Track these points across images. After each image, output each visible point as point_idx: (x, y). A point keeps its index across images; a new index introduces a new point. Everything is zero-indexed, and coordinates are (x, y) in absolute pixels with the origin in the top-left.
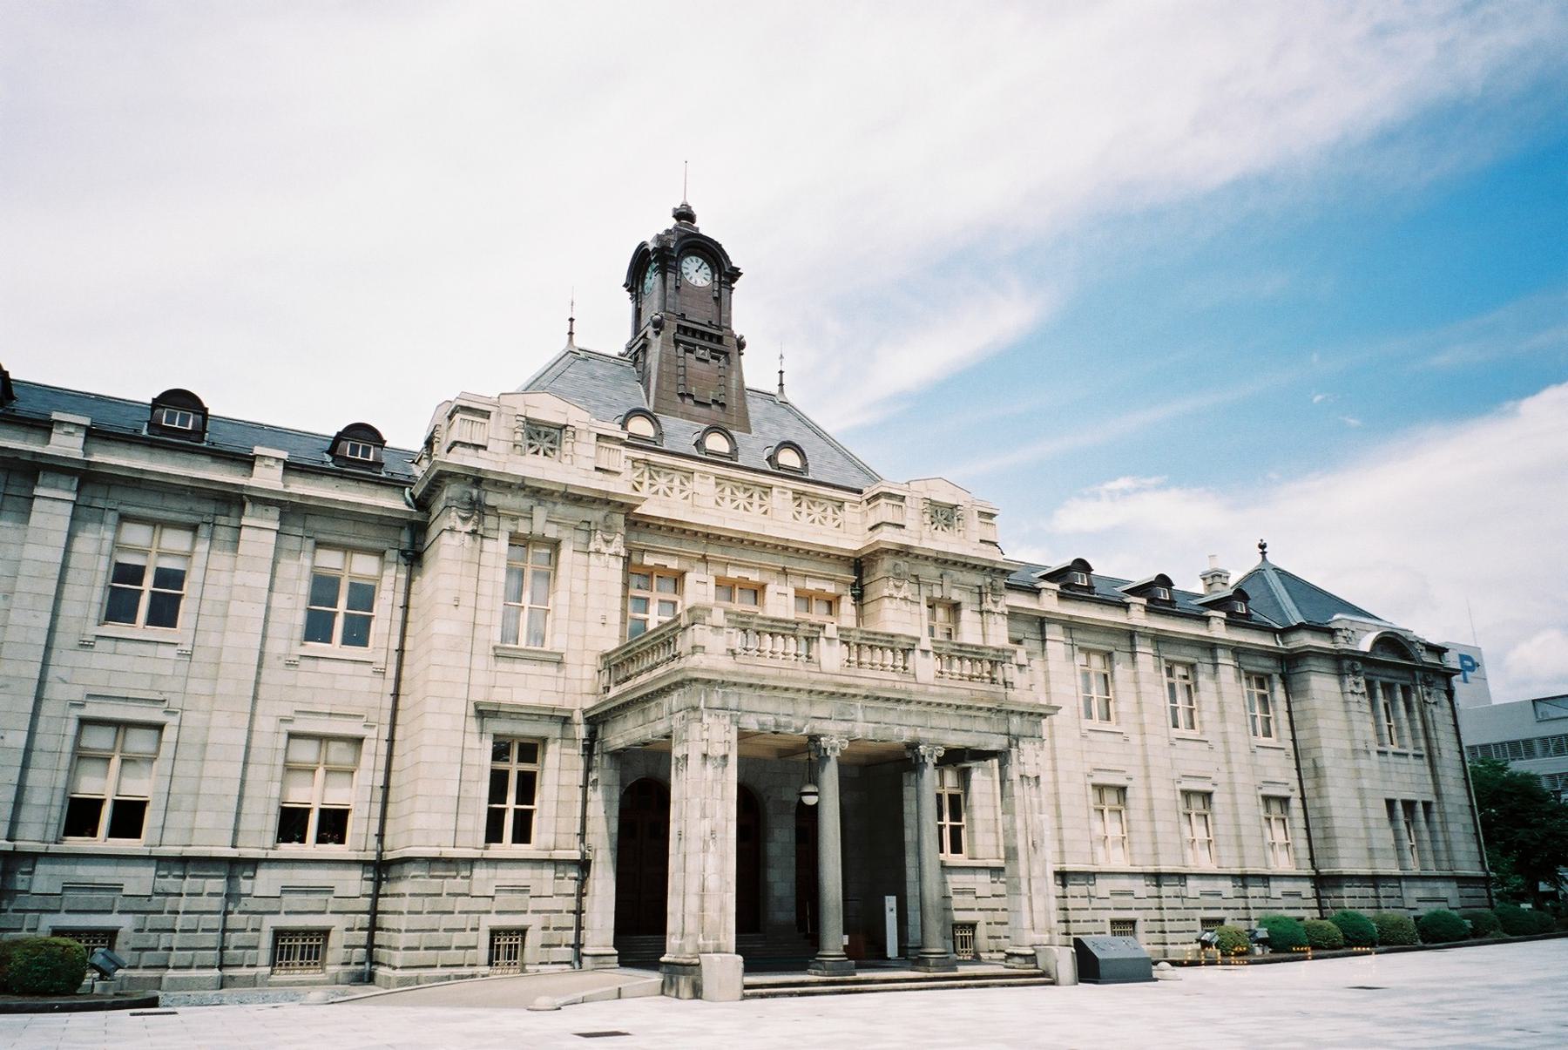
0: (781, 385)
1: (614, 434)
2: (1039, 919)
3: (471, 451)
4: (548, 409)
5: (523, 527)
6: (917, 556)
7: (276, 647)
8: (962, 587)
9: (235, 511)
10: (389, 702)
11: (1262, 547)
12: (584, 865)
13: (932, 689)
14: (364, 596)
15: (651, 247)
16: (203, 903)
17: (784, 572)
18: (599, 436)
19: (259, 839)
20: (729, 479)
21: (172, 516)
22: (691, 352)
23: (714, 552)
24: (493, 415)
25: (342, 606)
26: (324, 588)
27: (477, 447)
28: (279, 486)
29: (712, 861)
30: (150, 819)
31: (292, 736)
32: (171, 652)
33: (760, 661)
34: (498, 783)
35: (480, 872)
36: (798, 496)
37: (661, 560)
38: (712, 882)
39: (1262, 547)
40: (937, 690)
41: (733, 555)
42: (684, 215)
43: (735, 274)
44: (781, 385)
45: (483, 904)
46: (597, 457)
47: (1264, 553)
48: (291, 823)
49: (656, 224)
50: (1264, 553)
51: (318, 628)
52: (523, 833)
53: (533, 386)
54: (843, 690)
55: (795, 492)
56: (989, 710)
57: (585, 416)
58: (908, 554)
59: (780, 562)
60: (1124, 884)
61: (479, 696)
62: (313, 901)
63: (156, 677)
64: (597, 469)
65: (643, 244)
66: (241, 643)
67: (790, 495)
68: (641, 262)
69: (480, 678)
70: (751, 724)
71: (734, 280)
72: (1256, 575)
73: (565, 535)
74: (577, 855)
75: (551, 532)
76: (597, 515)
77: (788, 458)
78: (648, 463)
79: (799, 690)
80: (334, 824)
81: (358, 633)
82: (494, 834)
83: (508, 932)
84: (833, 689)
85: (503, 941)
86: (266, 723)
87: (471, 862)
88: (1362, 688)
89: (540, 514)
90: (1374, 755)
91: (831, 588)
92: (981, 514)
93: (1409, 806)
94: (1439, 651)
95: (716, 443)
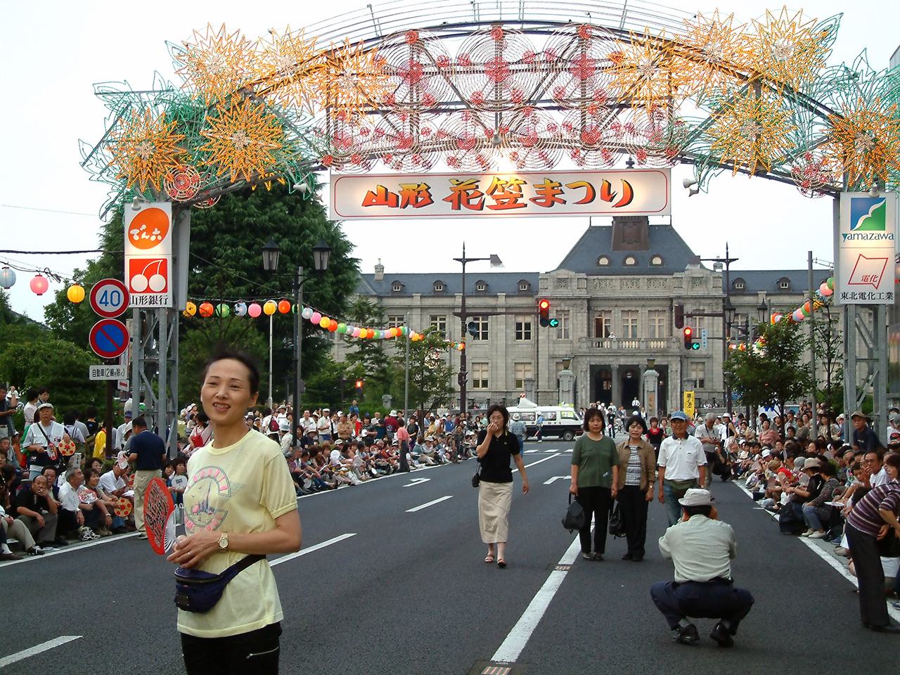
2: (674, 406)
4: (564, 274)
7: (510, 342)
8: (704, 305)
14: (528, 326)
19: (512, 387)
23: (620, 303)
26: (519, 326)
29: (584, 393)
31: (515, 363)
32: (487, 346)
37: (603, 309)
38: (584, 397)
41: (627, 303)
51: (519, 336)
53: (564, 265)
59: (643, 303)
66: (501, 342)
69: (551, 349)
73: (571, 308)
76: (579, 302)
77: (657, 261)
78: (598, 279)
81: (528, 336)
86: (510, 361)
91: (660, 309)
95: (630, 261)
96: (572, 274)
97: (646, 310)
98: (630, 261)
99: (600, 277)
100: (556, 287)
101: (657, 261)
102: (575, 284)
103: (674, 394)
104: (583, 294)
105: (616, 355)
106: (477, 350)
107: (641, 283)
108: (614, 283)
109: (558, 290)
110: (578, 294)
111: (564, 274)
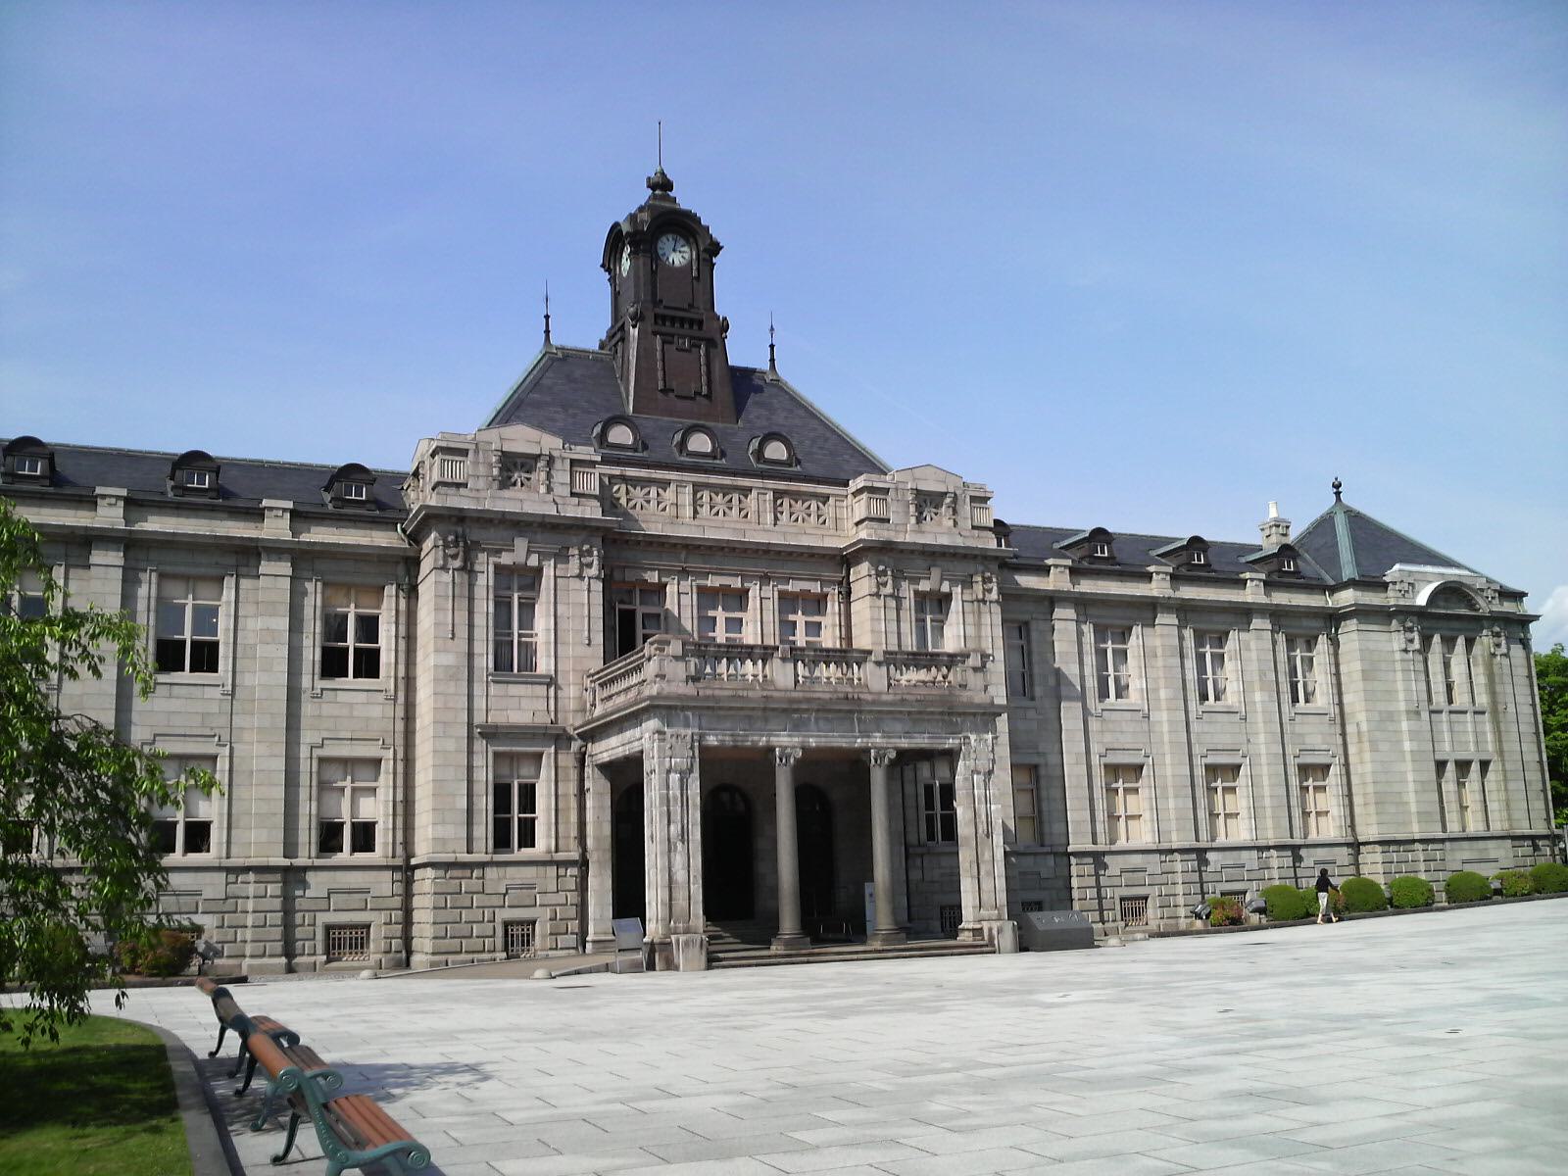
0: (772, 360)
1: (587, 458)
3: (453, 490)
4: (522, 438)
5: (506, 559)
6: (902, 551)
9: (253, 562)
10: (400, 726)
11: (1337, 486)
12: (583, 864)
13: (885, 698)
15: (626, 228)
16: (266, 904)
17: (765, 579)
18: (573, 462)
20: (707, 486)
21: (202, 571)
22: (671, 343)
24: (471, 454)
25: (351, 642)
26: (334, 627)
27: (458, 485)
28: (287, 536)
30: (216, 836)
33: (717, 684)
34: (501, 793)
35: (491, 873)
36: (778, 494)
39: (1337, 486)
40: (890, 698)
42: (662, 185)
43: (715, 248)
44: (772, 360)
45: (497, 901)
46: (572, 483)
47: (1338, 494)
48: (329, 837)
49: (629, 200)
50: (1338, 494)
51: (333, 664)
52: (528, 840)
54: (795, 706)
55: (775, 492)
56: (942, 713)
57: (558, 442)
58: (892, 550)
60: (1136, 860)
61: (479, 718)
62: (356, 900)
63: (205, 715)
64: (573, 494)
65: (616, 225)
67: (770, 496)
68: (616, 240)
69: (480, 703)
70: (712, 740)
71: (716, 254)
72: (1325, 524)
74: (575, 855)
75: (533, 561)
77: (776, 451)
79: (753, 709)
80: (364, 837)
81: (368, 665)
82: (502, 841)
83: (521, 923)
84: (785, 706)
85: (517, 931)
87: (483, 865)
88: (1417, 645)
89: (521, 544)
90: (1425, 715)
91: (815, 588)
92: (973, 499)
93: (1463, 766)
94: (1518, 596)
95: (700, 443)
96: (551, 443)
97: (770, 591)
98: (700, 443)
99: (631, 472)
100: (505, 483)
101: (776, 451)
102: (561, 476)
103: (987, 856)
104: (592, 511)
105: (790, 711)
106: (174, 705)
107: (751, 501)
108: (669, 495)
109: (506, 493)
110: (573, 510)
111: (522, 438)
